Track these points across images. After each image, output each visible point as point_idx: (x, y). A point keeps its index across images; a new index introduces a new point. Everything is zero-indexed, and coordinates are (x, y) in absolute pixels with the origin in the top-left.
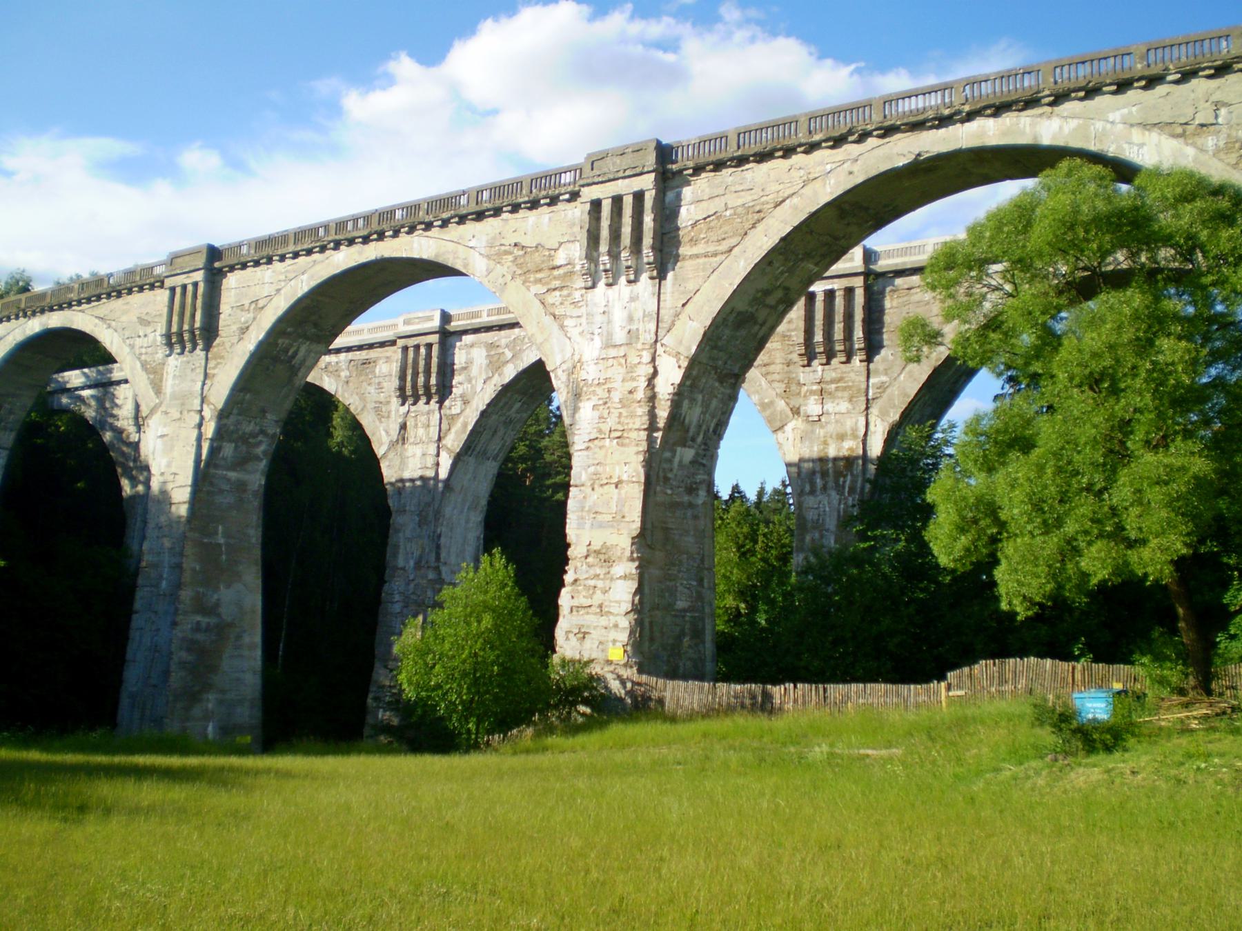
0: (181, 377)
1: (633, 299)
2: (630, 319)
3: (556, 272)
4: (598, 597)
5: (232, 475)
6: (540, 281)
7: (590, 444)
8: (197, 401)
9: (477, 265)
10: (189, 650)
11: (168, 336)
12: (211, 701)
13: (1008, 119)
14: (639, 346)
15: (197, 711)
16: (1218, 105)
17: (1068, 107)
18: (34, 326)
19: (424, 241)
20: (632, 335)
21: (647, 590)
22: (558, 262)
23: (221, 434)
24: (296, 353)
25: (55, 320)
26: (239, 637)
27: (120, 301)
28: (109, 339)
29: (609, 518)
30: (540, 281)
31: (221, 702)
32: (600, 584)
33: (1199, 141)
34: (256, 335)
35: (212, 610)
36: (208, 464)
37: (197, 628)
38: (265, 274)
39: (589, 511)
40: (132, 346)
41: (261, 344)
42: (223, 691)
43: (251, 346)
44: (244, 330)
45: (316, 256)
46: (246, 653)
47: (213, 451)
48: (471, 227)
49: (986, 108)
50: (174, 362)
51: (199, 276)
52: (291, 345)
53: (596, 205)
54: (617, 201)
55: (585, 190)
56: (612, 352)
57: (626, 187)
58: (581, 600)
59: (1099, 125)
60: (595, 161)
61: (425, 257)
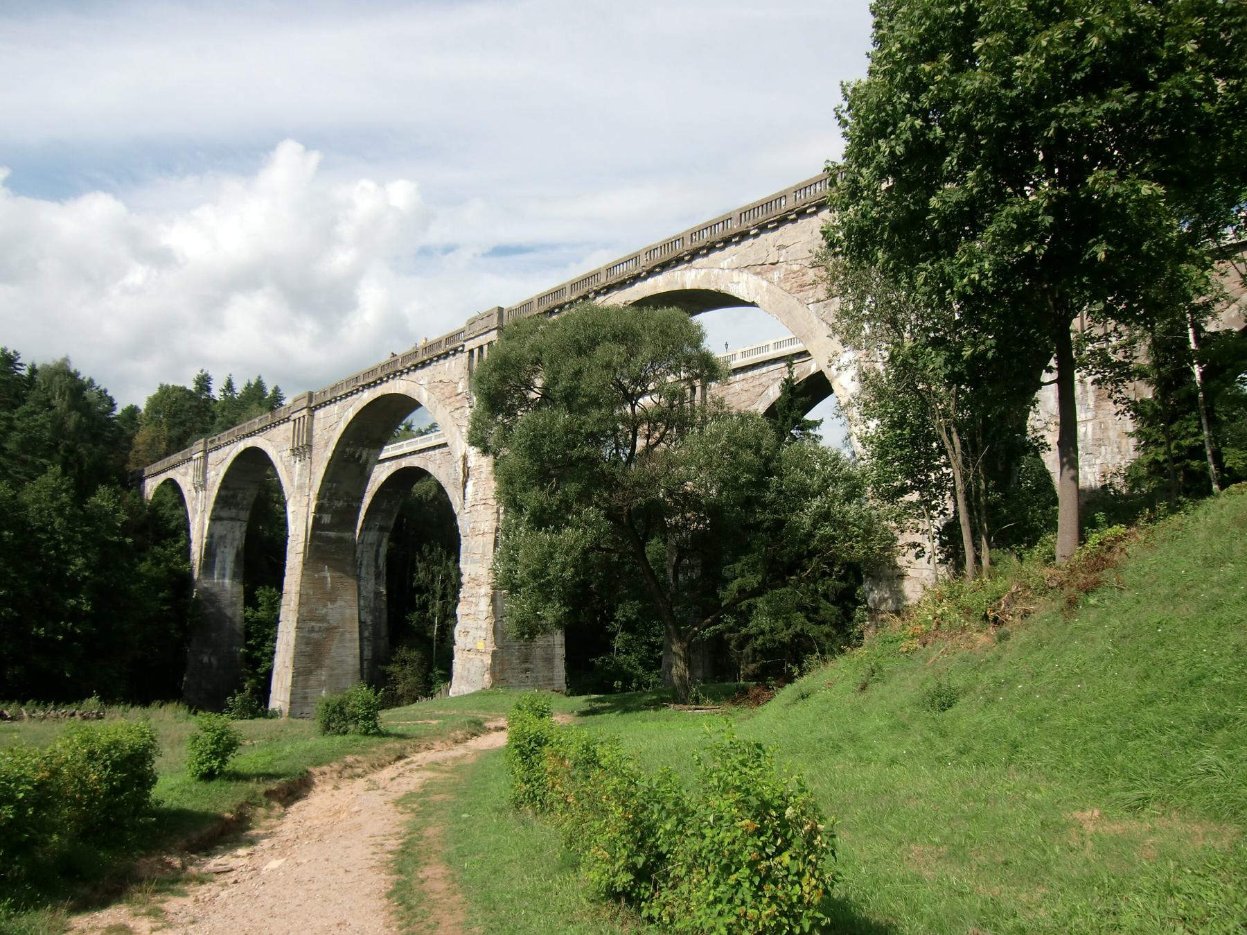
0: (300, 475)
4: (473, 609)
5: (332, 534)
9: (423, 396)
10: (307, 644)
11: (293, 450)
12: (323, 674)
13: (667, 275)
15: (313, 682)
16: (780, 247)
17: (698, 262)
21: (499, 603)
22: (460, 391)
23: (320, 509)
24: (360, 456)
26: (342, 634)
29: (477, 557)
31: (331, 675)
32: (474, 600)
33: (769, 275)
34: (332, 447)
35: (323, 619)
37: (312, 630)
38: (334, 408)
42: (333, 669)
46: (348, 644)
47: (316, 521)
48: (419, 373)
49: (655, 267)
50: (298, 466)
51: (305, 412)
52: (354, 453)
53: (471, 351)
54: (481, 348)
57: (483, 340)
58: (468, 612)
59: (716, 271)
60: (472, 323)
61: (401, 392)
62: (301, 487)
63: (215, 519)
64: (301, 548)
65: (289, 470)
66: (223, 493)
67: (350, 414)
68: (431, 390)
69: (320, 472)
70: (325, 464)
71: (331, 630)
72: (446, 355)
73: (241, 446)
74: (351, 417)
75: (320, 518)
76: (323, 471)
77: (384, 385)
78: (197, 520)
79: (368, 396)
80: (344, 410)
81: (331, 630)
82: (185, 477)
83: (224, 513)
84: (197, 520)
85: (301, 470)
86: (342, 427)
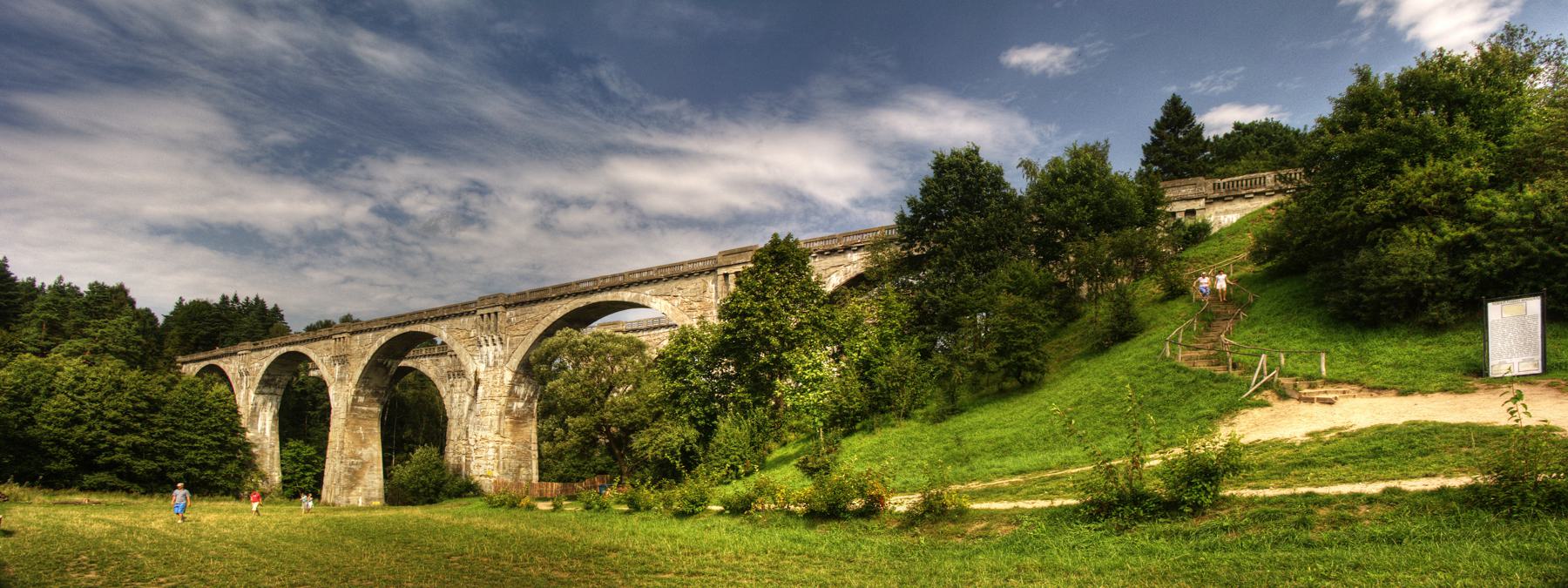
20: (496, 364)
23: (357, 393)
25: (292, 349)
28: (312, 355)
35: (359, 457)
47: (354, 401)
60: (482, 299)
62: (341, 380)
63: (258, 393)
64: (343, 415)
67: (383, 340)
71: (364, 464)
72: (461, 315)
73: (284, 350)
79: (397, 331)
81: (364, 464)
82: (231, 366)
83: (266, 390)
86: (376, 346)
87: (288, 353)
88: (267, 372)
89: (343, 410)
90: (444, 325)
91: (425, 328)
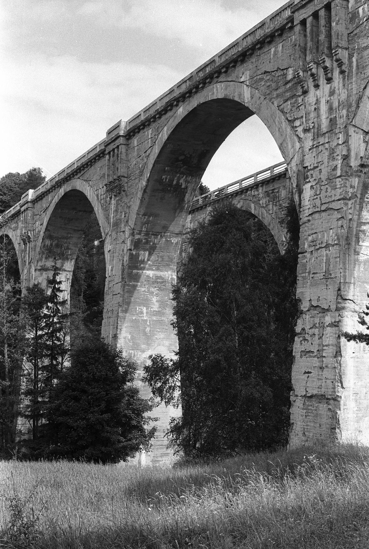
0: (116, 211)
1: (332, 93)
2: (331, 109)
3: (288, 86)
6: (278, 96)
7: (310, 218)
8: (123, 225)
14: (337, 131)
18: (62, 191)
19: (218, 85)
27: (93, 167)
29: (320, 276)
30: (278, 96)
36: (129, 267)
38: (149, 132)
39: (309, 272)
40: (97, 196)
41: (148, 180)
43: (144, 183)
44: (142, 173)
45: (169, 114)
52: (172, 181)
53: (303, 23)
55: (296, 14)
56: (322, 140)
62: (116, 224)
65: (106, 210)
66: (48, 242)
67: (165, 134)
68: (254, 84)
69: (135, 204)
70: (140, 195)
74: (166, 137)
75: (138, 255)
76: (138, 202)
77: (199, 95)
78: (25, 271)
80: (158, 131)
84: (25, 271)
85: (117, 204)
86: (157, 150)
87: (66, 194)
88: (49, 234)
89: (118, 279)
90: (244, 73)
91: (217, 91)
